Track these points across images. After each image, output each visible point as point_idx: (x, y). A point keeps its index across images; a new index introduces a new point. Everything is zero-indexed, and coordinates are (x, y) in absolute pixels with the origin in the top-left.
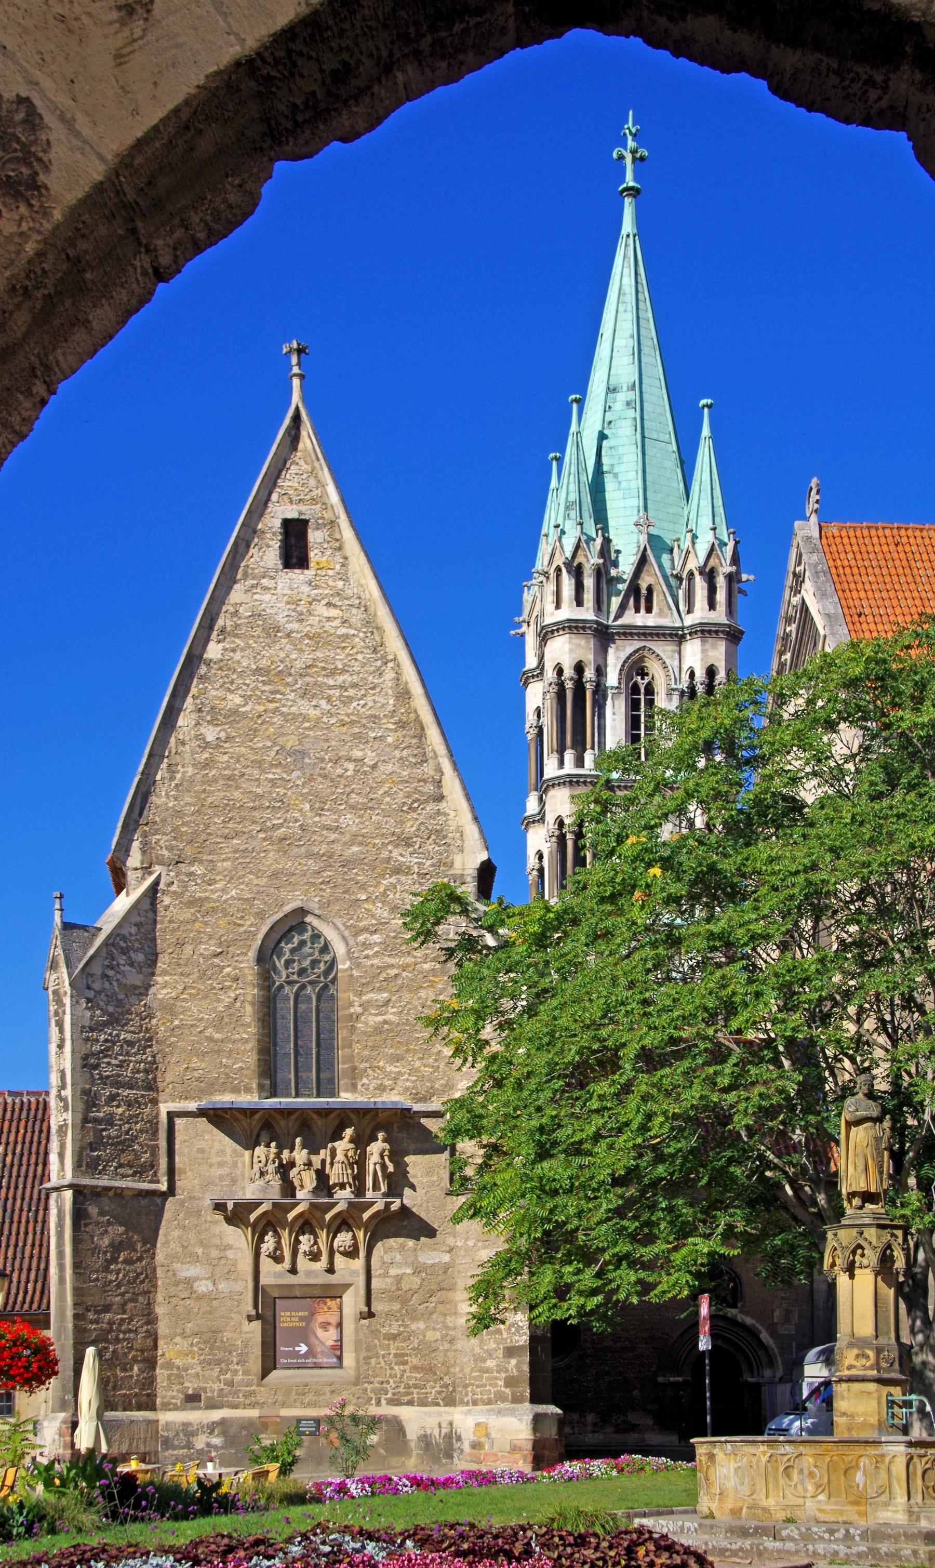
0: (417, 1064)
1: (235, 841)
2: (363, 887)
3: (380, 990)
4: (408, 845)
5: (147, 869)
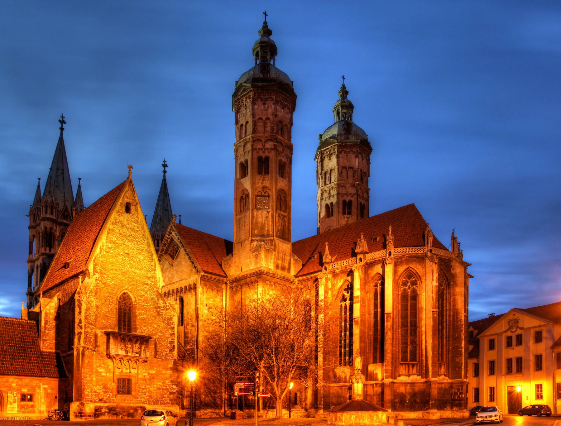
0: (149, 328)
1: (114, 271)
2: (140, 286)
3: (142, 310)
4: (149, 279)
5: (94, 274)
